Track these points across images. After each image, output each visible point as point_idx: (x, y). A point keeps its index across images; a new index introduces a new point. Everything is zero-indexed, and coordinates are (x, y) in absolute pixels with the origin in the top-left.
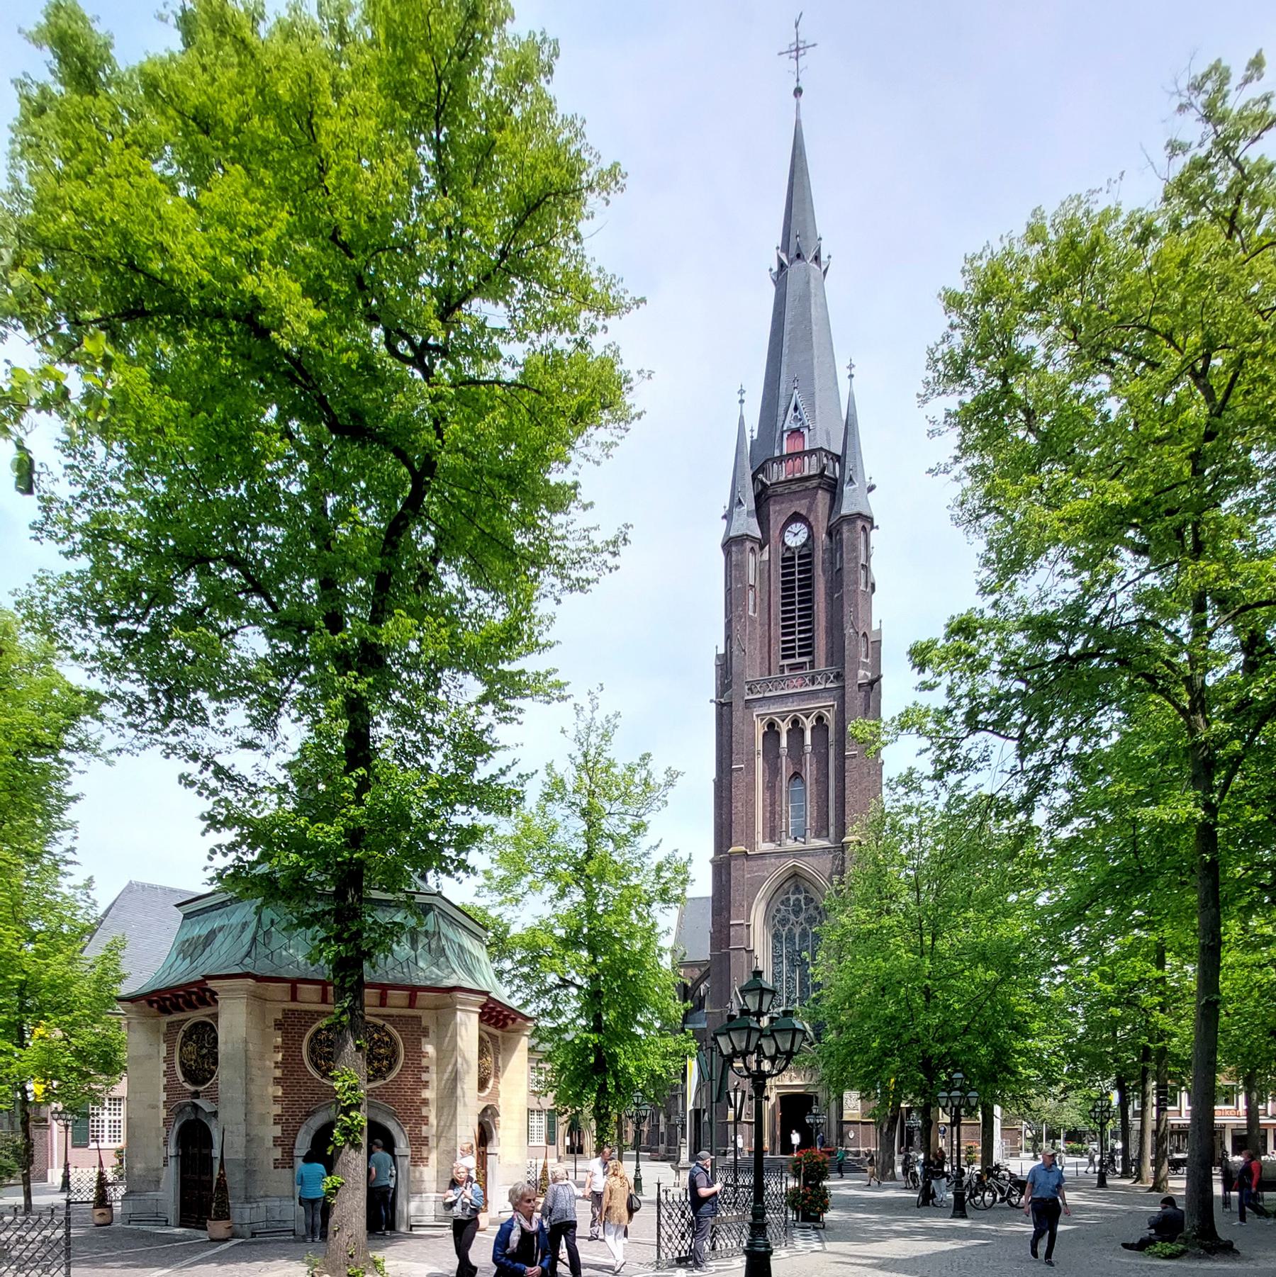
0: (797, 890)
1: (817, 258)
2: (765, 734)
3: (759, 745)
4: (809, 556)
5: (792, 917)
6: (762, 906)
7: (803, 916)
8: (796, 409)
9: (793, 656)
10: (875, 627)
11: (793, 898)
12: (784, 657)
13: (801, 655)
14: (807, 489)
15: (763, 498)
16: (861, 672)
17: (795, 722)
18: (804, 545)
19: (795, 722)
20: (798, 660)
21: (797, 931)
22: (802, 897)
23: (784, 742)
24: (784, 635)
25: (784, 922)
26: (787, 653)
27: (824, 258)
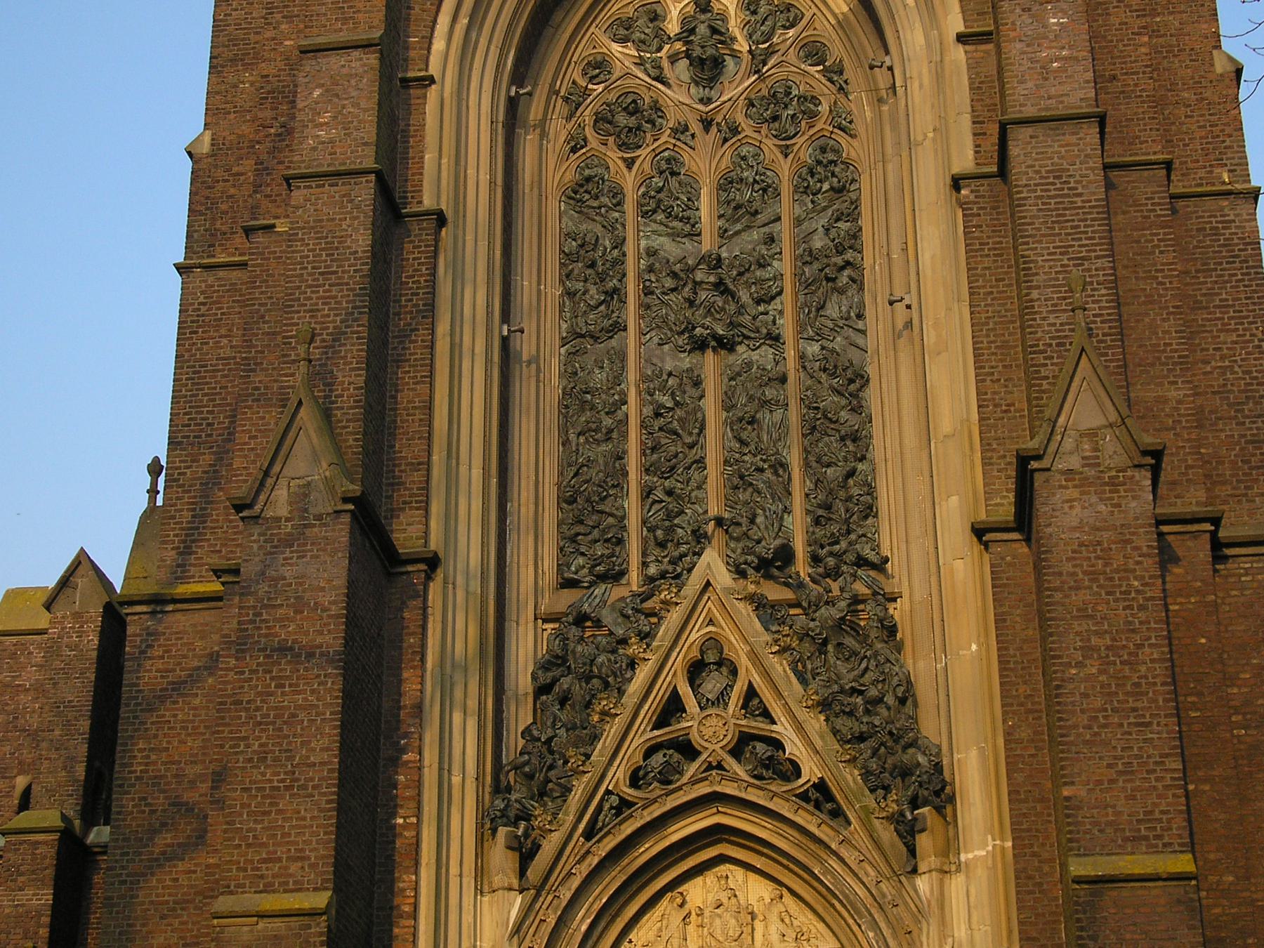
7: (736, 86)
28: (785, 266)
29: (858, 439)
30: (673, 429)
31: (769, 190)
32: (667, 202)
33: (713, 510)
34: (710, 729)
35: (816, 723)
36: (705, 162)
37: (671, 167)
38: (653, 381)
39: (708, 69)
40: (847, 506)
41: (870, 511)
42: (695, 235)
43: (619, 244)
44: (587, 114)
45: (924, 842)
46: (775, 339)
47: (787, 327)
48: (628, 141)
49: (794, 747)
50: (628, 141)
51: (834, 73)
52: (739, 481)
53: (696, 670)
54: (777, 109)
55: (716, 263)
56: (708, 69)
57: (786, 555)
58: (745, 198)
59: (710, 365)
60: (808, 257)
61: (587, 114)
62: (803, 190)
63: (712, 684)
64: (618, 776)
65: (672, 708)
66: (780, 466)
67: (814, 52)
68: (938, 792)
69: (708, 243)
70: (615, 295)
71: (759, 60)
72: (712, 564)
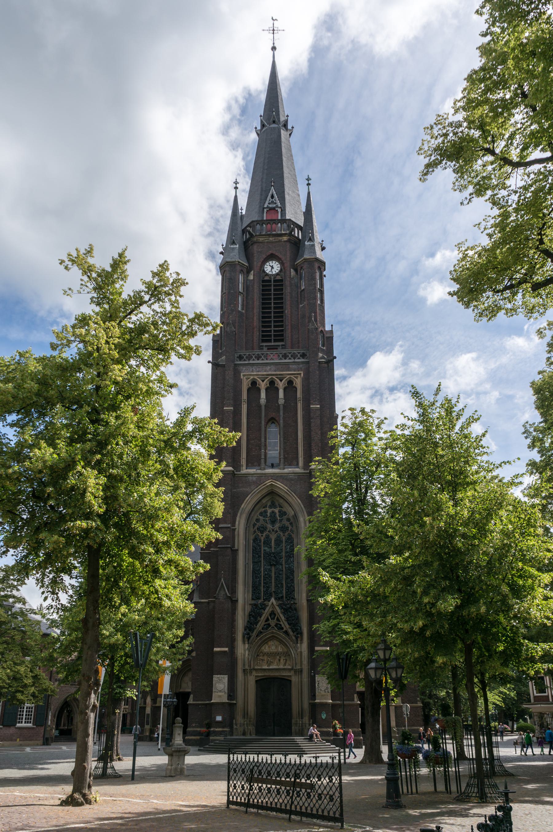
0: (273, 505)
1: (285, 125)
2: (249, 390)
3: (245, 396)
4: (281, 281)
5: (269, 526)
6: (244, 517)
7: (277, 525)
8: (272, 197)
9: (270, 341)
10: (328, 328)
11: (269, 511)
12: (263, 341)
13: (275, 341)
14: (280, 241)
15: (246, 246)
16: (320, 355)
17: (272, 382)
18: (277, 274)
19: (272, 382)
20: (273, 344)
21: (273, 537)
22: (277, 511)
23: (263, 395)
24: (263, 327)
25: (262, 529)
26: (265, 338)
27: (289, 127)
28: (283, 554)
29: (292, 580)
30: (268, 577)
31: (282, 542)
32: (267, 542)
33: (273, 590)
34: (273, 623)
35: (286, 623)
36: (273, 537)
37: (267, 537)
38: (265, 570)
39: (273, 522)
40: (291, 591)
41: (294, 591)
42: (271, 547)
43: (260, 549)
44: (256, 528)
45: (299, 639)
46: (282, 565)
47: (284, 563)
48: (262, 532)
49: (283, 626)
50: (262, 532)
51: (291, 524)
52: (276, 586)
53: (270, 615)
54: (283, 529)
55: (274, 553)
56: (273, 522)
57: (282, 597)
58: (278, 541)
59: (273, 569)
60: (286, 552)
61: (256, 528)
62: (286, 542)
63: (272, 616)
64: (261, 628)
65: (267, 620)
66: (282, 584)
67: (288, 520)
68: (301, 634)
69: (273, 551)
70: (260, 556)
71: (281, 521)
72: (273, 600)
